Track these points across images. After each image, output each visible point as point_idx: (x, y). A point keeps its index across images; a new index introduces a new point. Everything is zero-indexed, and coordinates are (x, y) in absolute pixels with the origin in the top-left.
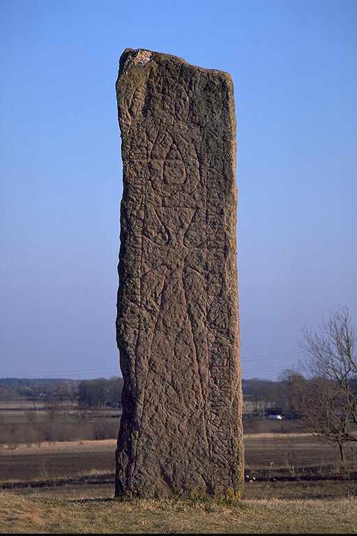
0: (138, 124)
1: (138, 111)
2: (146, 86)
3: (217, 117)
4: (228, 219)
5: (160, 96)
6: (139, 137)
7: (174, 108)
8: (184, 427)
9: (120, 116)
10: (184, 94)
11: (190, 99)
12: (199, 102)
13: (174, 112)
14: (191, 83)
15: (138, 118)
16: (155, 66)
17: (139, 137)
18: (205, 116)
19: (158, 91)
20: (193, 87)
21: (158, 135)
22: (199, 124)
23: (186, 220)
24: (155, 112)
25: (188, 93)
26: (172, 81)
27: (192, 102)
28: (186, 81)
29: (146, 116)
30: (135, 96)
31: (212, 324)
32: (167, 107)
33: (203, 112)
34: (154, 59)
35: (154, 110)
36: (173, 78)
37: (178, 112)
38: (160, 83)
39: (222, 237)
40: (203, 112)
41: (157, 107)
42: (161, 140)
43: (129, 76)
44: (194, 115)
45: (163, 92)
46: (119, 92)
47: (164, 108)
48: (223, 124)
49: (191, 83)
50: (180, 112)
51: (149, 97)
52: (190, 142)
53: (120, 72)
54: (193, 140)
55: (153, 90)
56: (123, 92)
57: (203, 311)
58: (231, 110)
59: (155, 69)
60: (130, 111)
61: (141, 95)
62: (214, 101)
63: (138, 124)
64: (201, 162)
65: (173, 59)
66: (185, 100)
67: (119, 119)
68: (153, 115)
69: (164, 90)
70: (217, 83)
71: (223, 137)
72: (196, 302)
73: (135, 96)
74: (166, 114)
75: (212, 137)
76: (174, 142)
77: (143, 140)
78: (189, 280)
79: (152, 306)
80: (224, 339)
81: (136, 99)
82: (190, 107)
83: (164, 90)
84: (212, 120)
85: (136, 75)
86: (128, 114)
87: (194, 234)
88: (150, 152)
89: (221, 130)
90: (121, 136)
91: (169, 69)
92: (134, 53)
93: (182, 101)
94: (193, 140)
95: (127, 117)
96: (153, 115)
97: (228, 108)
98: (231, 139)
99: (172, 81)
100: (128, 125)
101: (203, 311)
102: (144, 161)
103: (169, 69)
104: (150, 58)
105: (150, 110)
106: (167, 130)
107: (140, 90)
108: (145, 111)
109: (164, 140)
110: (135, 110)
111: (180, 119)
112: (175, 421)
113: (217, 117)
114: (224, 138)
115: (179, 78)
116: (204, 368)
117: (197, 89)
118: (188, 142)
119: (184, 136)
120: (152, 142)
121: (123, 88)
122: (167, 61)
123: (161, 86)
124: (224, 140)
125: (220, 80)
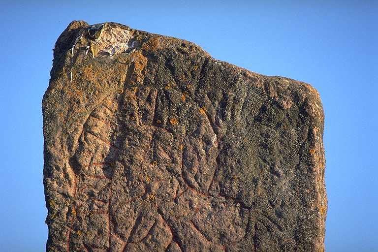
0: (91, 195)
1: (92, 162)
2: (116, 106)
3: (284, 184)
5: (147, 130)
6: (91, 224)
7: (179, 160)
9: (48, 172)
10: (206, 128)
11: (221, 139)
12: (242, 148)
13: (179, 169)
14: (224, 104)
15: (92, 181)
16: (140, 60)
17: (91, 224)
18: (255, 181)
19: (145, 119)
20: (229, 114)
21: (139, 221)
22: (238, 200)
24: (133, 167)
25: (215, 126)
26: (178, 97)
27: (225, 148)
28: (212, 96)
29: (110, 176)
30: (87, 129)
32: (164, 155)
33: (251, 170)
34: (139, 46)
35: (131, 162)
36: (183, 90)
37: (190, 168)
38: (149, 100)
40: (251, 170)
41: (139, 157)
42: (145, 233)
43: (78, 81)
44: (227, 176)
45: (157, 121)
46: (48, 117)
47: (155, 158)
48: (297, 201)
49: (224, 104)
50: (195, 169)
51: (123, 133)
52: (215, 239)
53: (55, 74)
54: (222, 236)
55: (132, 115)
56: (60, 119)
58: (317, 168)
59: (139, 68)
60: (75, 164)
61: (103, 127)
62: (277, 146)
63: (91, 195)
65: (184, 48)
66: (208, 142)
67: (45, 182)
68: (128, 174)
69: (158, 117)
70: (288, 104)
71: (296, 232)
73: (87, 129)
74: (160, 174)
75: (269, 229)
76: (176, 238)
77: (100, 232)
81: (89, 136)
82: (218, 160)
83: (158, 117)
84: (269, 191)
85: (93, 79)
86: (69, 170)
89: (291, 214)
90: (49, 221)
91: (173, 69)
92: (92, 33)
93: (201, 144)
94: (222, 236)
95: (66, 176)
96: (128, 174)
97: (310, 165)
98: (315, 235)
99: (178, 97)
100: (66, 195)
103: (173, 69)
104: (130, 43)
105: (123, 161)
106: (159, 211)
107: (101, 114)
108: (109, 165)
109: (151, 232)
110: (85, 161)
111: (192, 187)
113: (284, 184)
114: (299, 236)
115: (197, 91)
117: (238, 118)
118: (210, 239)
119: (202, 226)
120: (122, 237)
121: (61, 109)
122: (169, 50)
123: (151, 109)
124: (296, 238)
125: (296, 97)
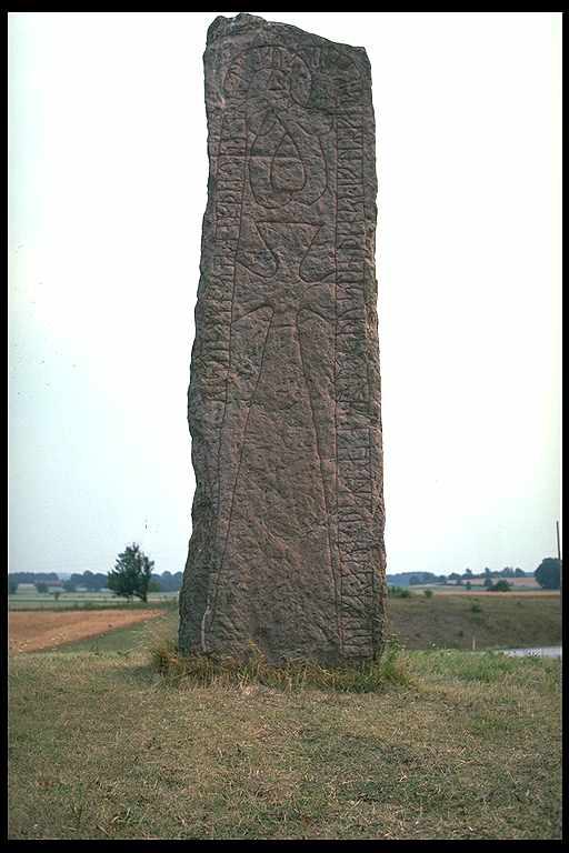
4: (367, 243)
8: (295, 554)
23: (304, 240)
31: (338, 393)
39: (358, 265)
57: (328, 375)
64: (328, 160)
72: (318, 360)
78: (305, 327)
79: (247, 367)
80: (362, 420)
87: (313, 259)
88: (250, 145)
100: (218, 109)
101: (328, 375)
102: (241, 158)
112: (281, 544)
116: (329, 463)
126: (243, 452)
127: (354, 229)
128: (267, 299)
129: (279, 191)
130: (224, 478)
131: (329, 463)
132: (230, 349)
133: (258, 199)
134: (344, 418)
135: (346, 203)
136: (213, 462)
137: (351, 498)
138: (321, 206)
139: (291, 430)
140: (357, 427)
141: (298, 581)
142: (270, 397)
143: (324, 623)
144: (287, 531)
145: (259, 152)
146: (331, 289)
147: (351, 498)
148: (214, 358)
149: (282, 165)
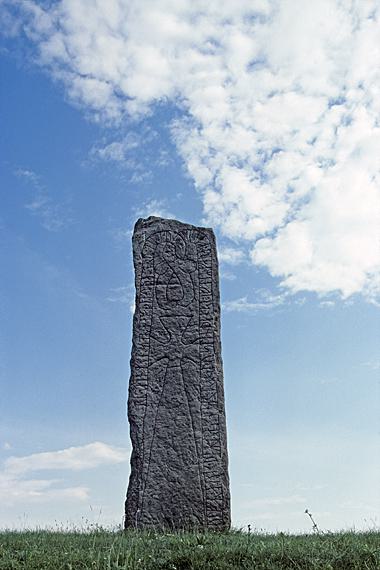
8: (182, 479)
64: (194, 284)
80: (215, 411)
116: (198, 433)
126: (155, 430)
127: (209, 317)
128: (165, 354)
129: (170, 301)
130: (146, 442)
131: (198, 433)
132: (148, 379)
133: (160, 305)
134: (206, 411)
135: (204, 304)
136: (140, 435)
137: (210, 450)
138: (192, 307)
139: (179, 418)
140: (212, 414)
141: (184, 493)
142: (168, 402)
143: (197, 513)
144: (179, 468)
145: (160, 283)
146: (198, 347)
147: (210, 450)
148: (140, 384)
149: (171, 288)
